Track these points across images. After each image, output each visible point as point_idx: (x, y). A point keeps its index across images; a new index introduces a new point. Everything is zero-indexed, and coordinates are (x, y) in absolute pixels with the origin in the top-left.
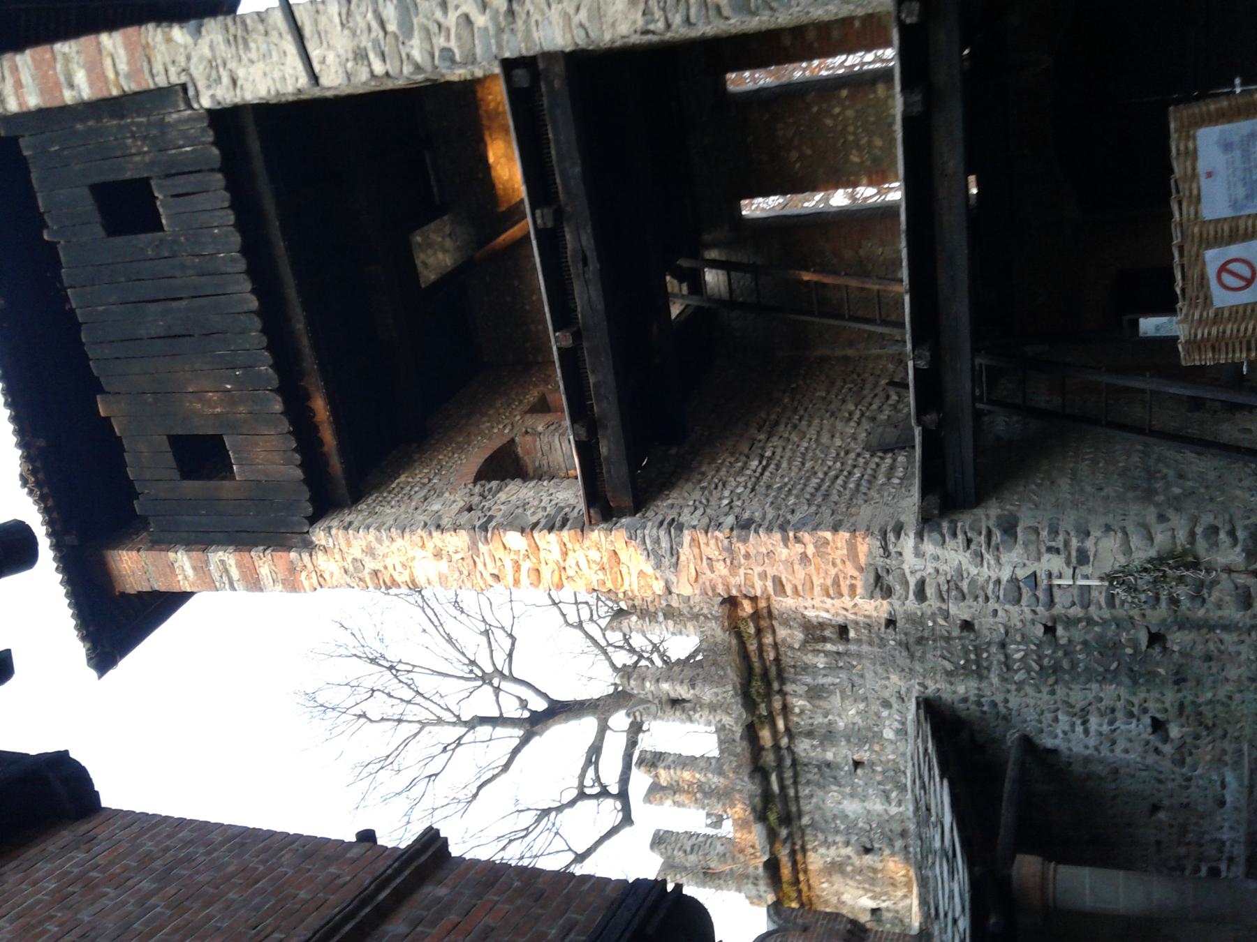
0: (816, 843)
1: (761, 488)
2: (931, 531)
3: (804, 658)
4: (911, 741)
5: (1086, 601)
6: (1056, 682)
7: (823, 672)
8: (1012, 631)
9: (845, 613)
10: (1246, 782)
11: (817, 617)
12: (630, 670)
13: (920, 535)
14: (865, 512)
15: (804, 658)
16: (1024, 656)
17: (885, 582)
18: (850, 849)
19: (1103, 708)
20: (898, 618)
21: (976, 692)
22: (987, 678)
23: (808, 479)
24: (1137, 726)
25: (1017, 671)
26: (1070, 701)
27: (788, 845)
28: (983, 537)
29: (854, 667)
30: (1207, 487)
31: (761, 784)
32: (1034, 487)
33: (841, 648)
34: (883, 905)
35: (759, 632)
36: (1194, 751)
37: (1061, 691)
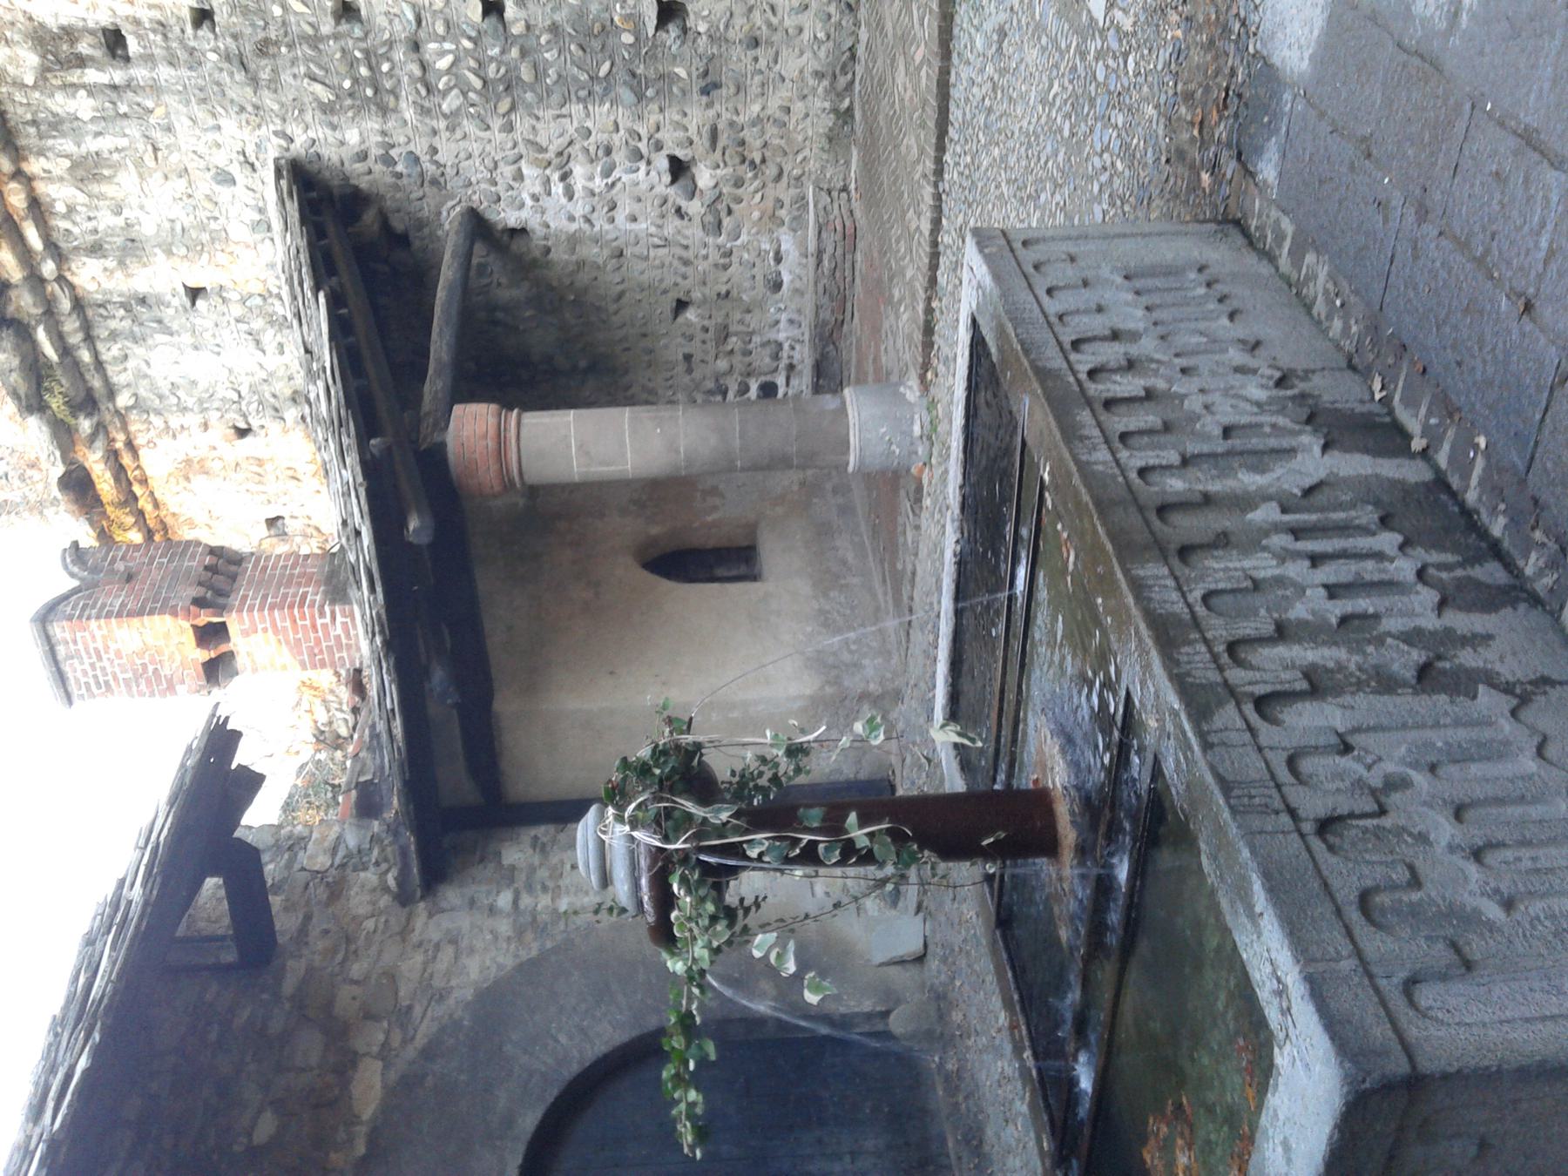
0: (152, 433)
3: (49, 102)
6: (513, 108)
7: (92, 128)
8: (427, 16)
10: (812, 246)
15: (49, 102)
16: (453, 64)
19: (592, 149)
21: (380, 139)
22: (396, 110)
24: (648, 174)
25: (445, 94)
26: (538, 139)
27: (100, 444)
31: (17, 348)
36: (733, 206)
37: (522, 124)
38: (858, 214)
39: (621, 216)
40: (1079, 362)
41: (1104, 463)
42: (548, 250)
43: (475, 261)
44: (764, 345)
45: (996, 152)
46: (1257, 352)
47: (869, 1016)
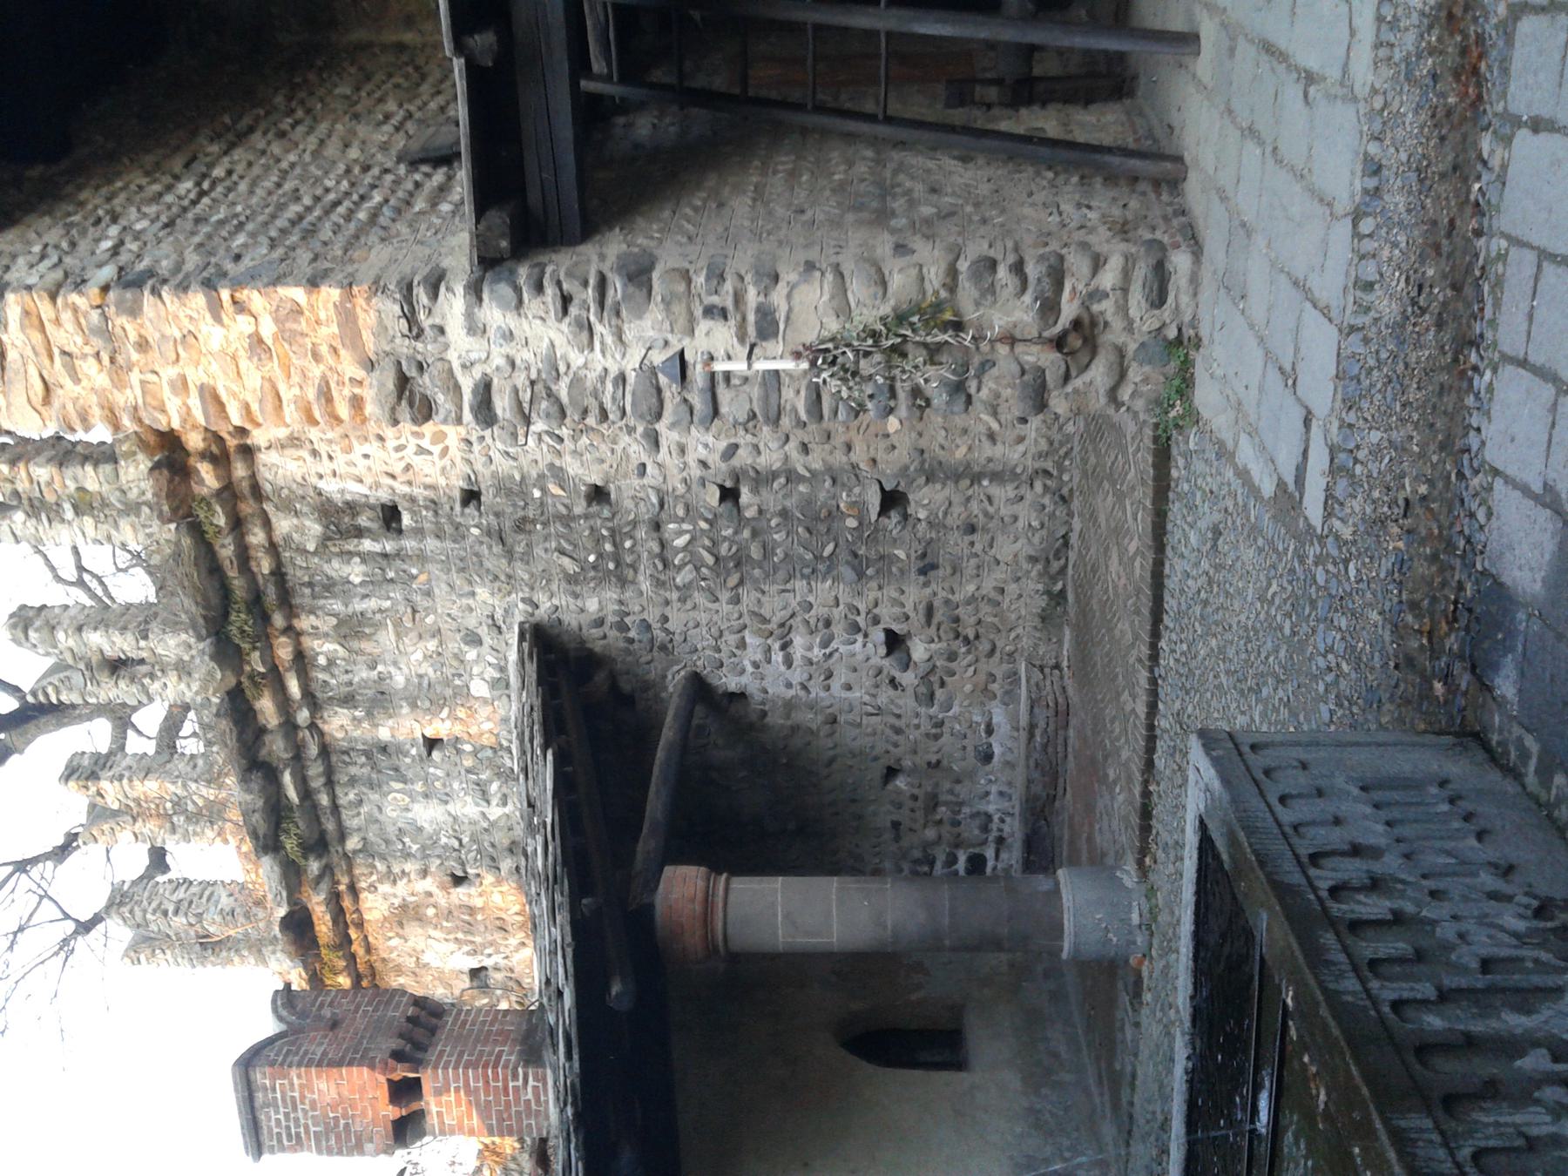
0: (374, 877)
1: (185, 224)
2: (497, 281)
3: (326, 567)
4: (514, 696)
5: (773, 413)
6: (741, 582)
7: (361, 590)
8: (669, 500)
9: (390, 481)
10: (1024, 720)
11: (342, 492)
12: (31, 614)
13: (475, 290)
14: (377, 255)
15: (326, 567)
16: (690, 542)
17: (417, 389)
18: (429, 879)
19: (813, 622)
20: (483, 487)
22: (633, 582)
23: (281, 207)
25: (680, 568)
27: (324, 886)
28: (590, 291)
29: (414, 577)
30: (977, 205)
31: (263, 790)
32: (688, 211)
33: (389, 546)
34: (488, 963)
35: (237, 524)
37: (748, 597)
38: (1070, 692)
39: (836, 685)
40: (1319, 878)
41: (1354, 993)
42: (764, 714)
43: (695, 722)
44: (974, 816)
45: (1214, 643)
46: (1510, 877)
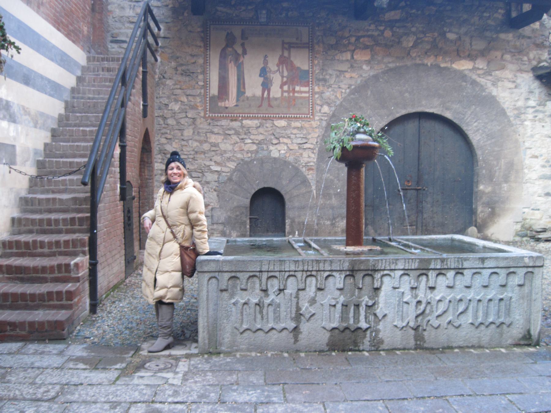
47: (476, 221)
